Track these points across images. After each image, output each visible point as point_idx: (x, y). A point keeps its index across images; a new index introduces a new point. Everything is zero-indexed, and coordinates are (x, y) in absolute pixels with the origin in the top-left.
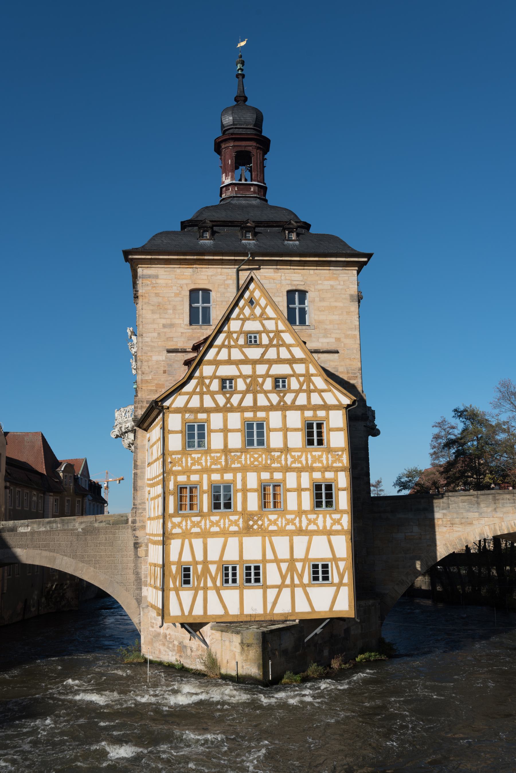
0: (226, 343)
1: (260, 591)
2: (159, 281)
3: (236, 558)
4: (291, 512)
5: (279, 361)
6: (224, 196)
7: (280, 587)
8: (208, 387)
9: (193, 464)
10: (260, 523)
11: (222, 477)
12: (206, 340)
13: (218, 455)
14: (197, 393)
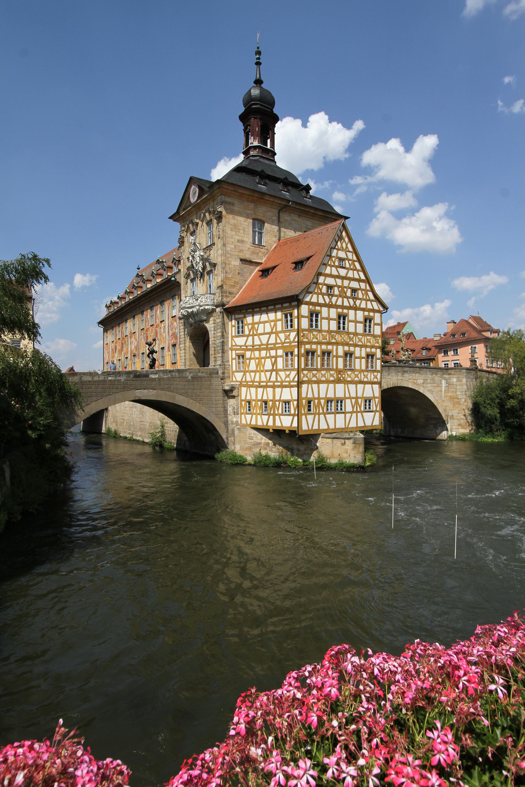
1: (343, 415)
2: (235, 208)
4: (357, 371)
6: (252, 153)
10: (344, 376)
11: (327, 348)
13: (326, 334)
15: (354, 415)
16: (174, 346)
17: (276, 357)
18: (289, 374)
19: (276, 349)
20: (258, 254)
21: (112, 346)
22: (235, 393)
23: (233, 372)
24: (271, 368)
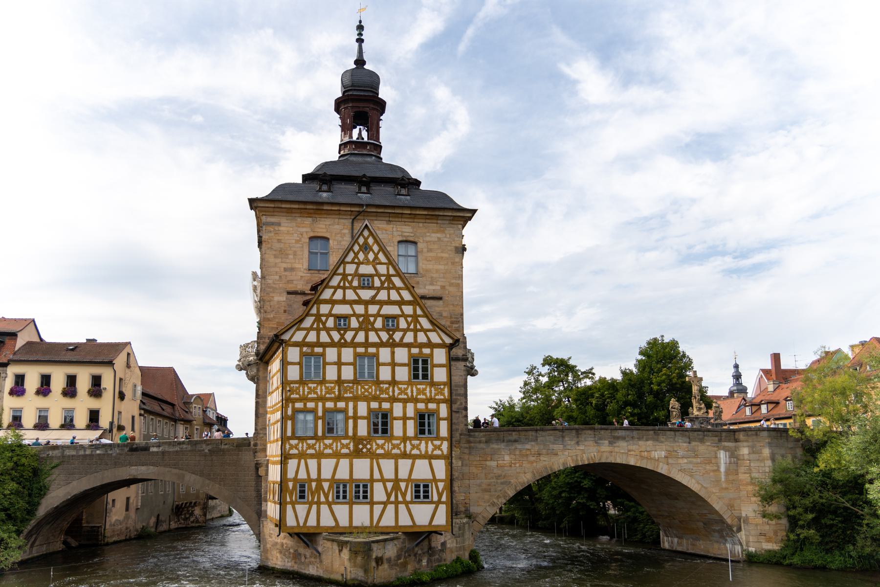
0: (342, 284)
1: (368, 507)
2: (281, 228)
3: (348, 477)
4: (397, 438)
5: (390, 302)
7: (385, 504)
8: (324, 324)
9: (309, 393)
10: (369, 446)
11: (335, 405)
12: (323, 281)
15: (391, 508)
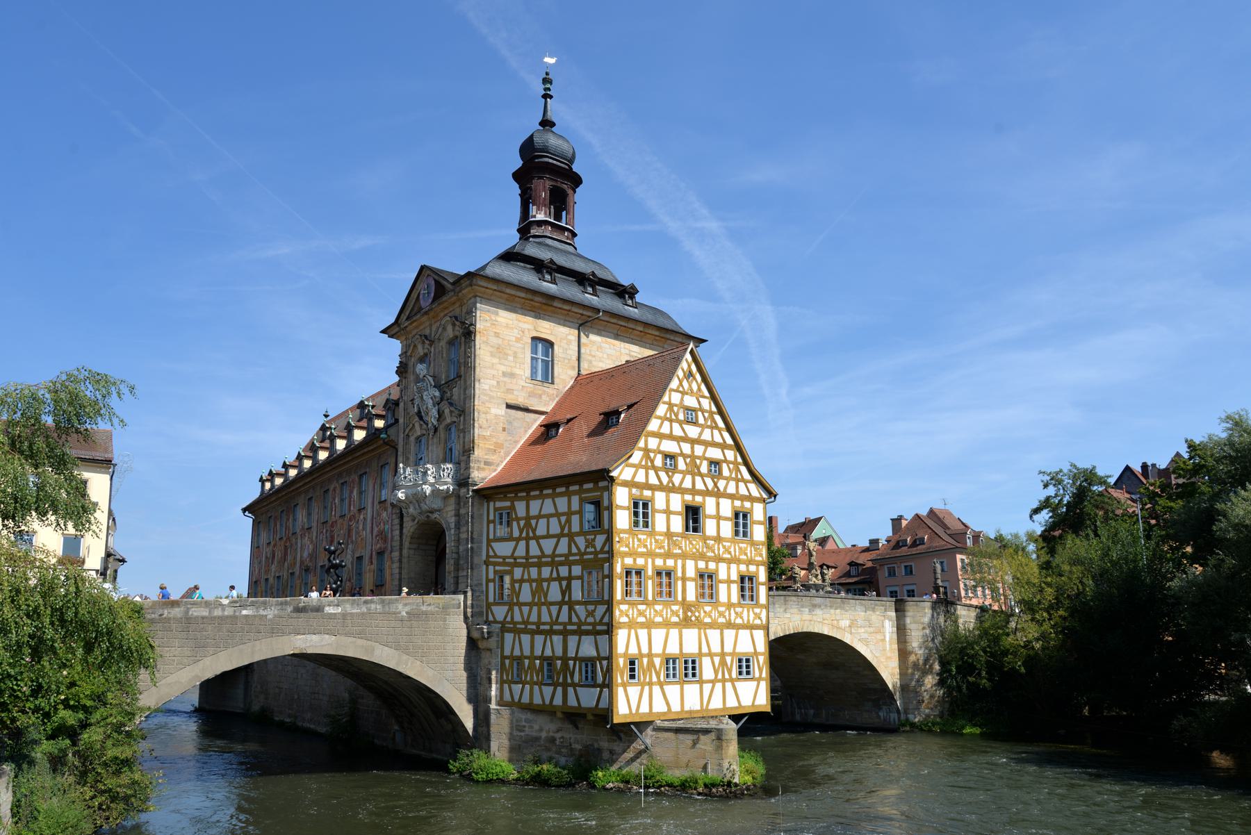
3: (677, 651)
14: (642, 467)
16: (380, 554)
17: (570, 579)
18: (594, 611)
19: (570, 564)
20: (540, 396)
21: (267, 551)
22: (492, 643)
23: (489, 606)
24: (559, 598)
